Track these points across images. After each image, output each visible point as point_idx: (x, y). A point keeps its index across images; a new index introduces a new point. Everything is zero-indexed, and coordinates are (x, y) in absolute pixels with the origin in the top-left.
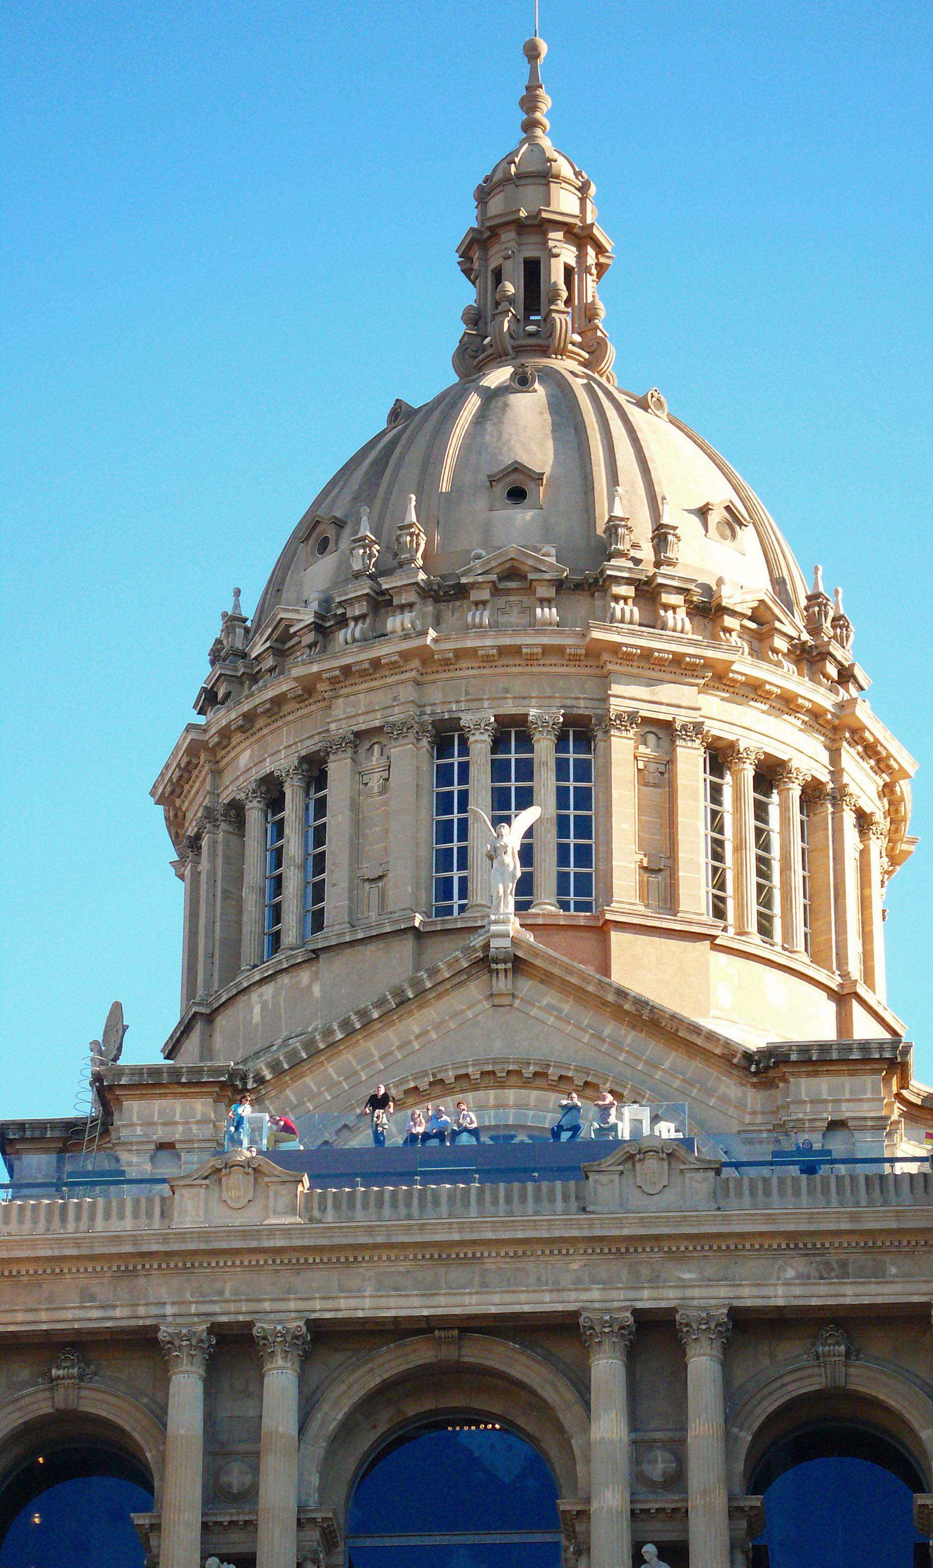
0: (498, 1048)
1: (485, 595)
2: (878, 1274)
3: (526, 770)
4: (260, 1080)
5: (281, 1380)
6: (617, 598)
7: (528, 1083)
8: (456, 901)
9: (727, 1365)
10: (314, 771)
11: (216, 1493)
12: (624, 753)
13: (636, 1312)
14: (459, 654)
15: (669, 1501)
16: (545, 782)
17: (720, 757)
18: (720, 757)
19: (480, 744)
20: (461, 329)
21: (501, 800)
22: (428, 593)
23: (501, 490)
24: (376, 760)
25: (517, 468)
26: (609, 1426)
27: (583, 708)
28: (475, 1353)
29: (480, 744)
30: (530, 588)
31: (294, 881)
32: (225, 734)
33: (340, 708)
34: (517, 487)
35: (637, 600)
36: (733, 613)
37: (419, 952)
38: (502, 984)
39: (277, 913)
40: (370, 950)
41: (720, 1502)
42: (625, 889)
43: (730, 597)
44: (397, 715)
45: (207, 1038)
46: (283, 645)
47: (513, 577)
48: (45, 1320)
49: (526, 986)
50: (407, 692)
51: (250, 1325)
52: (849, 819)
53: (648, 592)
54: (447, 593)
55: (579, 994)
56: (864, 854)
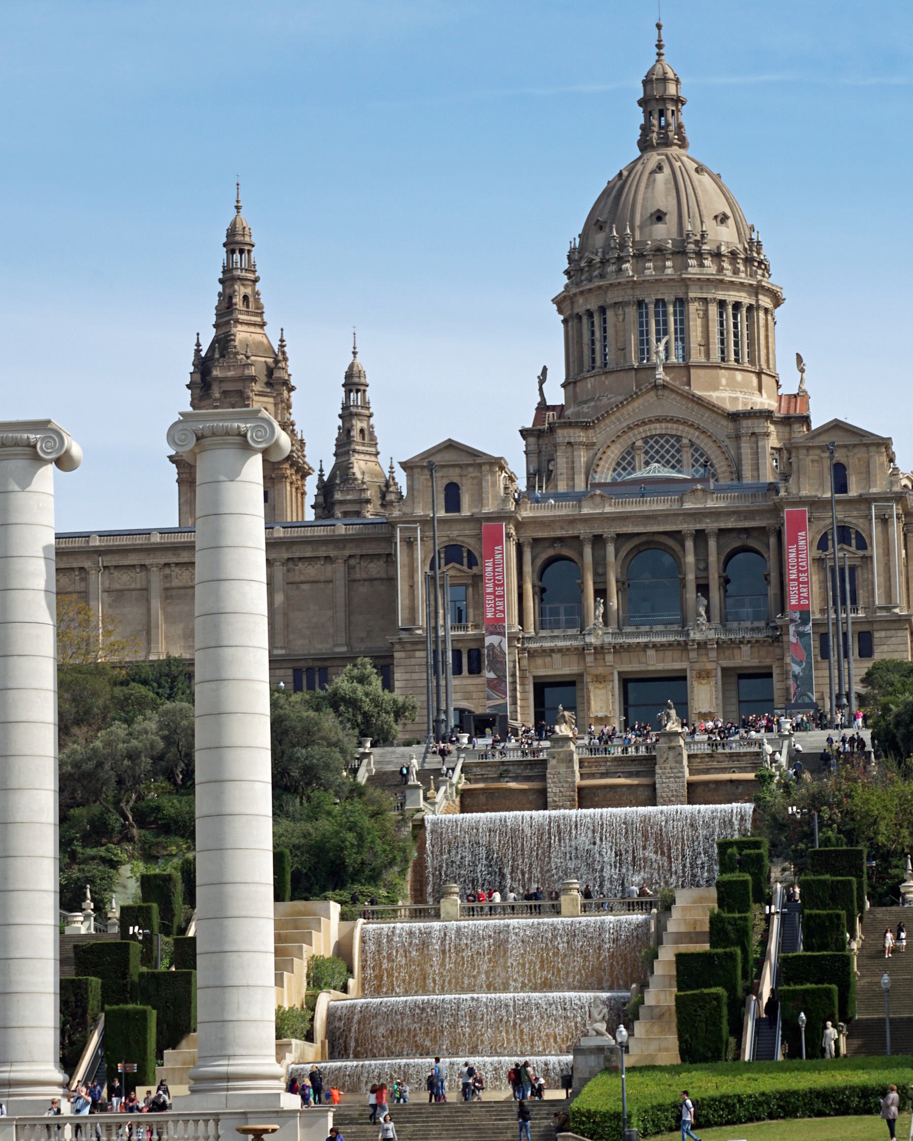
0: (659, 412)
1: (651, 257)
2: (754, 519)
3: (665, 314)
4: (593, 422)
5: (611, 549)
6: (690, 258)
7: (668, 422)
8: (646, 356)
9: (718, 543)
10: (603, 310)
11: (596, 574)
12: (693, 307)
13: (697, 531)
14: (644, 281)
15: (703, 574)
17: (722, 304)
20: (640, 132)
21: (657, 323)
22: (634, 256)
23: (654, 218)
24: (620, 312)
25: (659, 211)
26: (690, 559)
27: (681, 295)
28: (656, 538)
29: (651, 307)
30: (664, 255)
31: (598, 346)
32: (575, 295)
33: (610, 295)
34: (659, 217)
35: (696, 259)
36: (724, 256)
37: (636, 374)
38: (660, 392)
39: (593, 351)
40: (621, 374)
41: (716, 576)
43: (724, 249)
44: (626, 299)
45: (575, 388)
46: (590, 262)
47: (659, 251)
48: (553, 534)
49: (666, 393)
50: (629, 292)
51: (602, 535)
52: (762, 315)
53: (699, 255)
54: (640, 256)
55: (682, 395)
56: (767, 320)
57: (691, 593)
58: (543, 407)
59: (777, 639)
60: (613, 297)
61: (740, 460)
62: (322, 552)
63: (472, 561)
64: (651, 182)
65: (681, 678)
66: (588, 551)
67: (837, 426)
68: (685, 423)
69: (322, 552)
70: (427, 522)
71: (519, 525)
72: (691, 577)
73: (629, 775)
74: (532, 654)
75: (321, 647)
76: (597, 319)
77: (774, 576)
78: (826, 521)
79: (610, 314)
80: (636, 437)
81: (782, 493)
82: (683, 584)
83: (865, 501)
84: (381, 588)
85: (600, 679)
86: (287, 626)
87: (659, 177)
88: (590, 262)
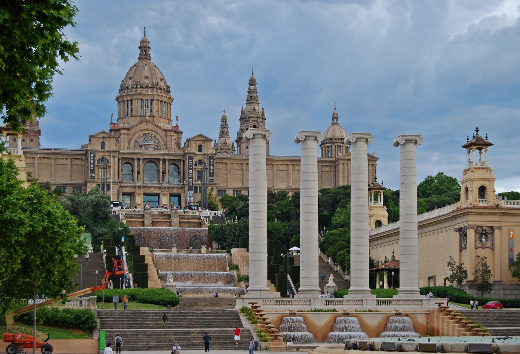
3: (148, 103)
5: (141, 162)
10: (131, 100)
16: (149, 104)
17: (161, 101)
18: (161, 101)
19: (145, 101)
26: (161, 166)
29: (145, 101)
31: (129, 109)
34: (147, 78)
39: (128, 111)
42: (155, 114)
46: (128, 87)
47: (147, 86)
53: (157, 88)
54: (142, 87)
57: (161, 175)
58: (111, 123)
59: (184, 187)
60: (134, 97)
61: (167, 141)
62: (65, 157)
63: (108, 162)
64: (144, 68)
65: (158, 195)
66: (136, 162)
67: (201, 135)
68: (153, 131)
69: (65, 157)
70: (97, 151)
71: (119, 153)
72: (161, 170)
73: (163, 219)
74: (122, 187)
75: (64, 181)
76: (129, 102)
77: (182, 172)
78: (196, 159)
79: (133, 101)
80: (141, 133)
81: (186, 151)
82: (158, 171)
83: (207, 154)
84: (80, 167)
85: (139, 194)
86: (55, 175)
87: (146, 67)
88: (128, 87)
